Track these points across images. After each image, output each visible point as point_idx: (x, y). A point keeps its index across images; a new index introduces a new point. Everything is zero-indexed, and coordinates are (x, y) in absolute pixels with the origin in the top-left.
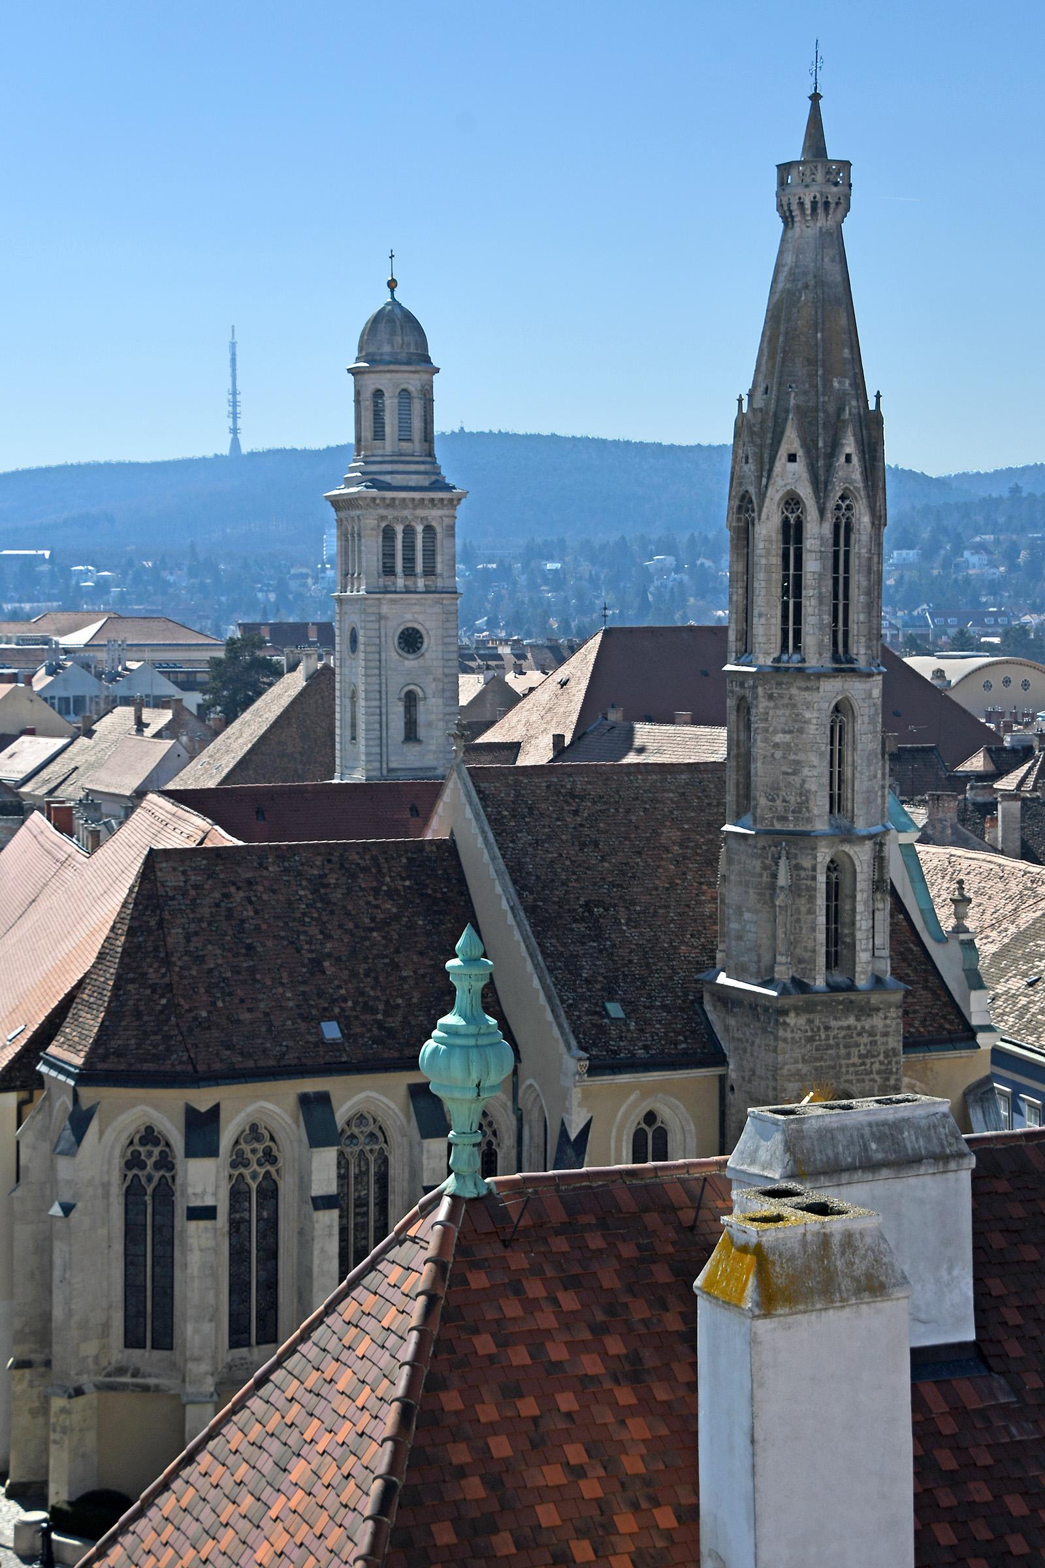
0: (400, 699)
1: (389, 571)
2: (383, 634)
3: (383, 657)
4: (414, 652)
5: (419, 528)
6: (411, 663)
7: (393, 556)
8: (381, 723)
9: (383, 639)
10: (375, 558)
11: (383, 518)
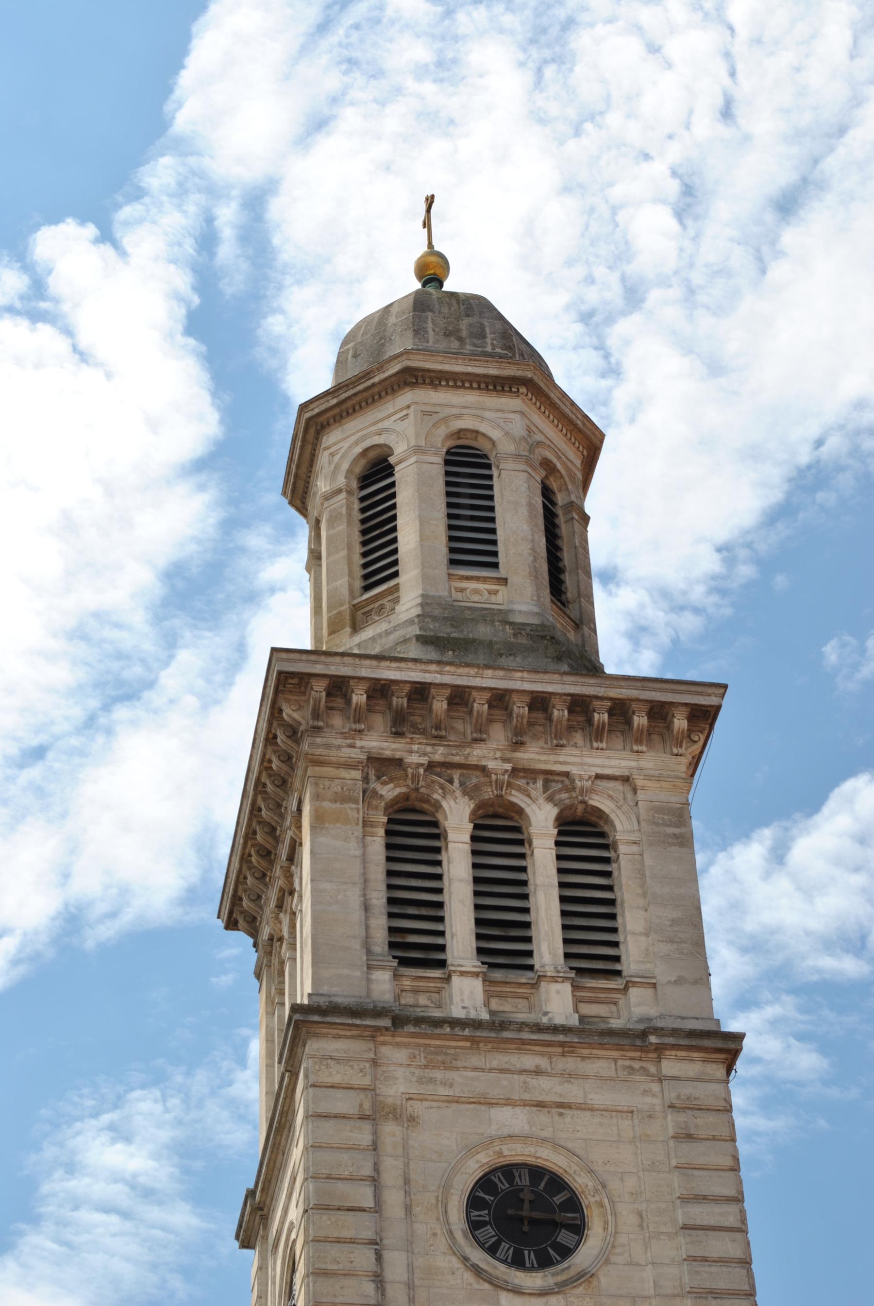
1: (415, 947)
2: (391, 1175)
3: (396, 1265)
4: (544, 1262)
5: (541, 820)
7: (435, 911)
9: (394, 1199)
10: (354, 897)
11: (383, 766)
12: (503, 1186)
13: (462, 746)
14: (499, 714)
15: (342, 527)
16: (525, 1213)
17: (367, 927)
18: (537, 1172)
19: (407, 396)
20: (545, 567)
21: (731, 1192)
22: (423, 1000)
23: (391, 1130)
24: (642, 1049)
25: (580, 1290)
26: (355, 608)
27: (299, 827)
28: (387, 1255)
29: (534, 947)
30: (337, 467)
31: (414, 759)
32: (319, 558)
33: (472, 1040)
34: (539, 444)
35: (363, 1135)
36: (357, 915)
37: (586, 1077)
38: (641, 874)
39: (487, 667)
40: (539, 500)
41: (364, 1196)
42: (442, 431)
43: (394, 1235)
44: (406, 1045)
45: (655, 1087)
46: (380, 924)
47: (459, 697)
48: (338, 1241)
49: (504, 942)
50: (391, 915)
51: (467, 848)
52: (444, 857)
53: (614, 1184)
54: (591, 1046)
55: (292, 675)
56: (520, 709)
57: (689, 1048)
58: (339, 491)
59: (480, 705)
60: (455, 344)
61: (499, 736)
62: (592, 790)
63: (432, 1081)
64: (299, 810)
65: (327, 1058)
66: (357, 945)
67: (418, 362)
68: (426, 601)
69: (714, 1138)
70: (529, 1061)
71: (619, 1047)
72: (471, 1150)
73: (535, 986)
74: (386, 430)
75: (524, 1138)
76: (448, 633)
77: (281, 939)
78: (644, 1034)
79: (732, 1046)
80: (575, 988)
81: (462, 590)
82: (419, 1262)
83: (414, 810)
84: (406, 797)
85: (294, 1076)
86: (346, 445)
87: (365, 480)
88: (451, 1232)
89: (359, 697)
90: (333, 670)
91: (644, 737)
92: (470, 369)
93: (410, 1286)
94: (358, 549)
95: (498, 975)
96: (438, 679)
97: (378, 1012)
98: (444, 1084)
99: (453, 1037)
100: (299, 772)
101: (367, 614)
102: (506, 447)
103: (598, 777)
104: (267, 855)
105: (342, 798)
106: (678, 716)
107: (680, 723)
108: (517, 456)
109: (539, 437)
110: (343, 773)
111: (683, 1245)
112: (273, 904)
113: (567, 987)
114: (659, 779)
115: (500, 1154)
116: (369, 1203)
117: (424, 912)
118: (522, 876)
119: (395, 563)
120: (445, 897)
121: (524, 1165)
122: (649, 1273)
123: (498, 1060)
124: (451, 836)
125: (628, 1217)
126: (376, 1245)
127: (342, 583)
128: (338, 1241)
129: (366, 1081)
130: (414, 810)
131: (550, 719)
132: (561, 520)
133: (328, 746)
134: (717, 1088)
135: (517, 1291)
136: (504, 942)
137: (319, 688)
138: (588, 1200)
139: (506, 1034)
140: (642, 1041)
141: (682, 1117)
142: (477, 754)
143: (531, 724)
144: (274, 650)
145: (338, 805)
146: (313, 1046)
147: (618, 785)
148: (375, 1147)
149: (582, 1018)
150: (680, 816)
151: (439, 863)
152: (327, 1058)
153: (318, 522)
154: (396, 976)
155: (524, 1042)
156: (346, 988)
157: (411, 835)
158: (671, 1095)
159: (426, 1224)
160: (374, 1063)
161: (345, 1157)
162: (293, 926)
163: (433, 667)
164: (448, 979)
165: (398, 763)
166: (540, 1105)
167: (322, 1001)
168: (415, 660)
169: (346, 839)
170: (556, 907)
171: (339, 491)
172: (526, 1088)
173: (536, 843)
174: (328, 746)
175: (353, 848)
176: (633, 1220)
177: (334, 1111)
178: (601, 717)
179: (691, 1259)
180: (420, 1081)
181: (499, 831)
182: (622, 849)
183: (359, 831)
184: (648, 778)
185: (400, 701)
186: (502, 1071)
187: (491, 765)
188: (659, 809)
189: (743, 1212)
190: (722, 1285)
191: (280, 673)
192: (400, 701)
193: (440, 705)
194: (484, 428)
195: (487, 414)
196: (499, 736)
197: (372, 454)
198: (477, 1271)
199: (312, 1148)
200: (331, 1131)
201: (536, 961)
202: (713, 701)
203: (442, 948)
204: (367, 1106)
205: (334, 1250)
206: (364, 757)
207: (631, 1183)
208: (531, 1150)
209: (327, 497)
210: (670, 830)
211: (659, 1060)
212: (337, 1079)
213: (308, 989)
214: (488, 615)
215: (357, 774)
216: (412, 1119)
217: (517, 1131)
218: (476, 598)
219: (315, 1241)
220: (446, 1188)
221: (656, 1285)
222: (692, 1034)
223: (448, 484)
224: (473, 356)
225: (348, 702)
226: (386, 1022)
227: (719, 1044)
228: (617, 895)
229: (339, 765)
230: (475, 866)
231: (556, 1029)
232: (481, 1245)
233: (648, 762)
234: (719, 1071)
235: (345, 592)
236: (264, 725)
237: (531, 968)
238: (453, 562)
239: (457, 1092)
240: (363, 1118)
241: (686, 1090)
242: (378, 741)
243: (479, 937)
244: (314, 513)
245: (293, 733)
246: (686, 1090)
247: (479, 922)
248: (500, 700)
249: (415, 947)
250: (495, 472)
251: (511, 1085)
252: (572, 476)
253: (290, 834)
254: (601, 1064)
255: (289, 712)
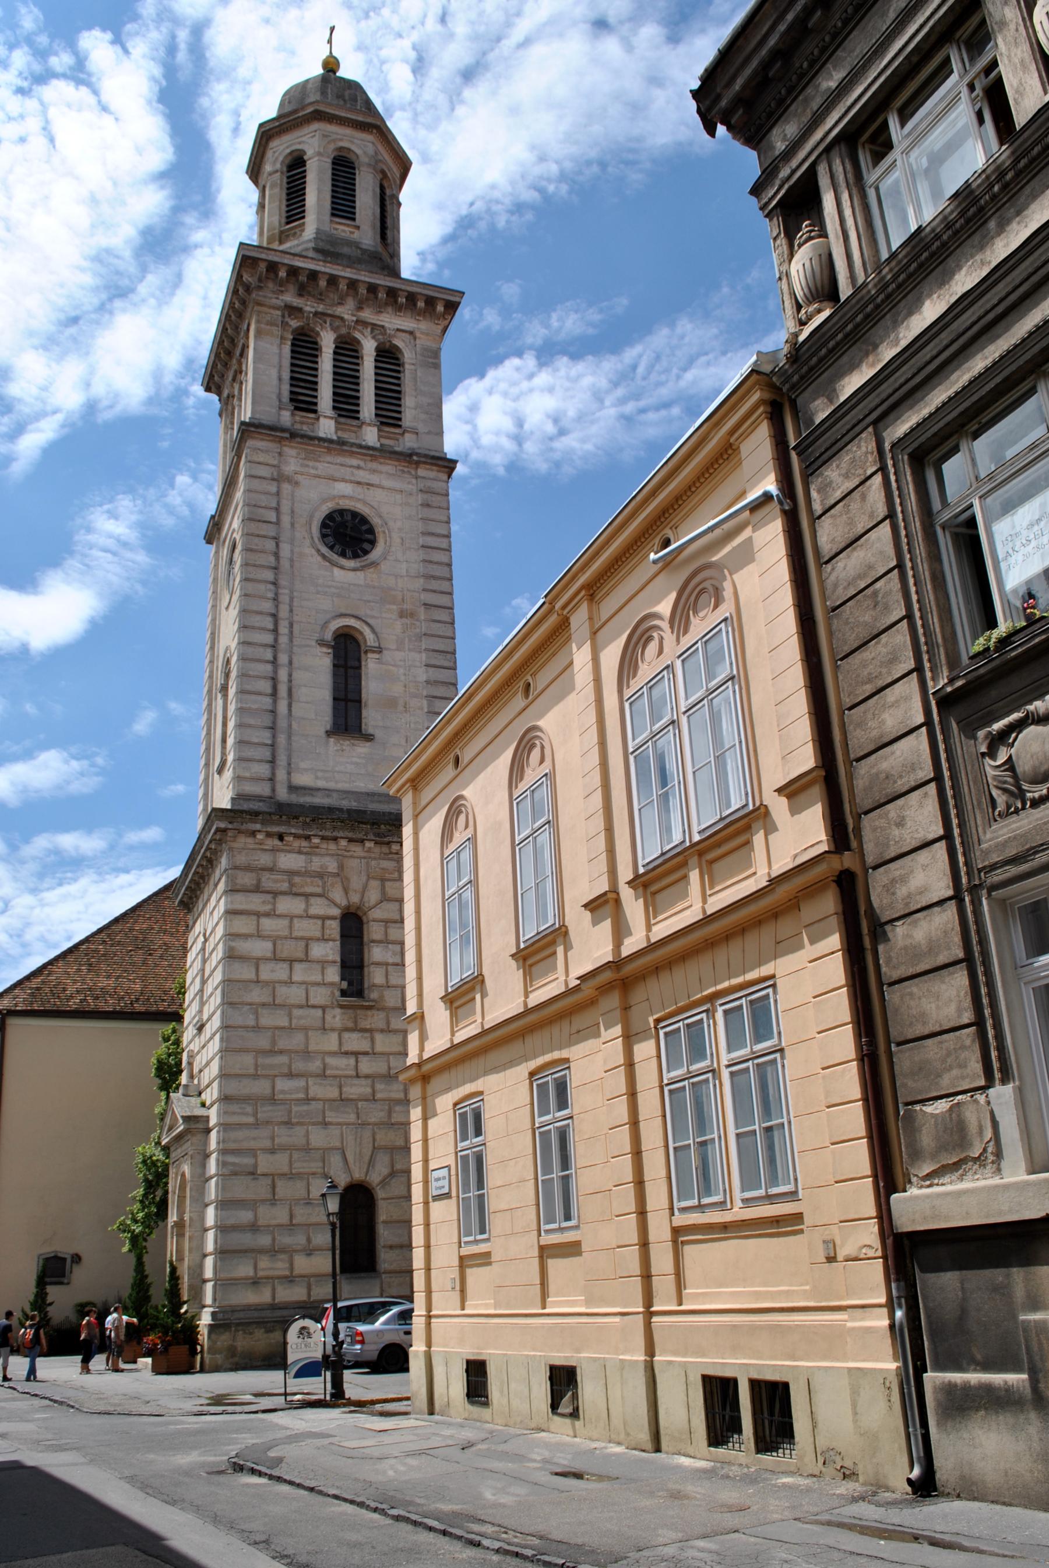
0: (321, 643)
1: (302, 400)
2: (285, 508)
3: (285, 550)
4: (355, 556)
5: (369, 347)
6: (345, 575)
7: (313, 386)
8: (274, 680)
9: (286, 519)
11: (292, 310)
12: (338, 519)
13: (333, 305)
14: (351, 292)
15: (277, 190)
16: (348, 532)
17: (280, 389)
18: (355, 514)
19: (315, 126)
20: (378, 224)
21: (445, 533)
22: (305, 428)
23: (286, 487)
24: (410, 462)
25: (371, 570)
26: (281, 232)
27: (247, 338)
28: (281, 545)
29: (360, 409)
30: (277, 159)
31: (308, 309)
32: (264, 207)
33: (328, 448)
34: (380, 161)
35: (273, 489)
36: (275, 382)
37: (381, 472)
38: (415, 379)
39: (348, 267)
40: (378, 190)
41: (272, 516)
42: (332, 146)
43: (285, 536)
44: (296, 448)
45: (414, 481)
46: (286, 388)
47: (333, 280)
48: (258, 536)
49: (346, 404)
50: (291, 385)
51: (331, 356)
52: (319, 360)
53: (391, 524)
54: (385, 458)
55: (249, 257)
56: (363, 291)
57: (432, 464)
58: (277, 171)
59: (343, 286)
60: (342, 103)
61: (351, 303)
62: (394, 336)
63: (307, 466)
64: (248, 329)
65: (256, 449)
66: (274, 397)
67: (322, 108)
68: (318, 232)
69: (439, 507)
70: (355, 462)
71: (398, 460)
72: (324, 501)
73: (360, 427)
74: (304, 142)
75: (351, 498)
76: (328, 248)
77: (233, 397)
78: (411, 455)
79: (451, 465)
80: (379, 430)
81: (336, 229)
82: (297, 550)
83: (306, 335)
84: (302, 328)
85: (239, 458)
86: (282, 148)
87: (291, 167)
88: (312, 538)
89: (282, 274)
90: (270, 258)
91: (422, 313)
92: (349, 116)
93: (292, 560)
94: (284, 203)
95: (342, 420)
96: (323, 269)
97: (283, 430)
98: (313, 468)
99: (320, 446)
100: (249, 310)
101: (288, 236)
102: (364, 159)
103: (398, 330)
104: (229, 354)
105: (271, 323)
106: (438, 304)
107: (440, 308)
108: (369, 165)
109: (380, 157)
110: (272, 311)
111: (422, 554)
112: (230, 378)
113: (375, 429)
114: (427, 334)
115: (338, 504)
116: (274, 520)
117: (308, 385)
118: (357, 374)
119: (304, 211)
120: (319, 380)
121: (349, 510)
122: (404, 566)
123: (340, 459)
124: (324, 349)
125: (396, 540)
126: (276, 539)
127: (276, 219)
128: (258, 536)
129: (275, 462)
130: (306, 335)
131: (377, 298)
132: (388, 202)
133: (265, 297)
134: (444, 484)
135: (342, 568)
136: (346, 404)
137: (263, 266)
138: (378, 530)
139: (345, 448)
140: (411, 459)
141: (425, 496)
142: (339, 311)
143: (367, 299)
144: (241, 244)
145: (268, 327)
146: (250, 443)
147: (407, 335)
148: (278, 494)
149: (381, 445)
150: (436, 354)
151: (317, 363)
152: (256, 449)
153: (264, 187)
154: (293, 415)
155: (353, 452)
156: (269, 414)
157: (304, 348)
158: (421, 486)
159: (300, 533)
160: (280, 454)
161: (263, 497)
162: (240, 390)
163: (321, 263)
164: (318, 419)
165: (300, 310)
166: (359, 483)
167: (256, 421)
168: (312, 259)
169: (272, 344)
170: (372, 391)
171: (277, 171)
172: (353, 474)
173: (365, 358)
174: (265, 297)
175: (275, 349)
176: (399, 540)
177: (260, 474)
178: (402, 300)
179: (424, 561)
180: (302, 465)
181: (347, 351)
182: (407, 366)
183: (278, 341)
184: (422, 333)
185: (303, 278)
186: (342, 465)
187: (346, 317)
188: (426, 349)
189: (450, 542)
190: (437, 574)
191: (243, 256)
192: (303, 278)
193: (323, 283)
194: (353, 148)
195: (356, 141)
196: (351, 303)
197: (295, 154)
198: (324, 557)
199: (248, 491)
200: (256, 484)
201: (361, 416)
202: (457, 299)
203: (316, 404)
204: (275, 474)
205: (256, 540)
206: (283, 304)
207: (399, 524)
208: (353, 503)
209: (270, 174)
210: (431, 360)
211: (417, 468)
212: (261, 460)
213: (249, 414)
214: (349, 243)
215: (279, 313)
216: (297, 483)
217: (346, 494)
218: (343, 234)
219: (247, 535)
220: (311, 517)
221: (407, 571)
222: (433, 457)
223: (333, 174)
224: (350, 110)
225: (277, 275)
226: (287, 435)
227: (446, 464)
228: (403, 389)
229: (270, 307)
230: (334, 366)
231: (369, 448)
232: (326, 545)
233: (422, 326)
234: (445, 477)
235: (277, 224)
236: (233, 284)
237: (358, 419)
238: (333, 215)
239: (319, 472)
240: (273, 479)
241: (429, 483)
242: (290, 297)
243: (334, 401)
244: (261, 182)
245: (248, 289)
246: (429, 483)
247: (334, 394)
248: (353, 284)
249: (302, 400)
250: (357, 172)
251: (346, 472)
252: (395, 181)
253: (242, 341)
254: (389, 467)
255: (246, 277)
